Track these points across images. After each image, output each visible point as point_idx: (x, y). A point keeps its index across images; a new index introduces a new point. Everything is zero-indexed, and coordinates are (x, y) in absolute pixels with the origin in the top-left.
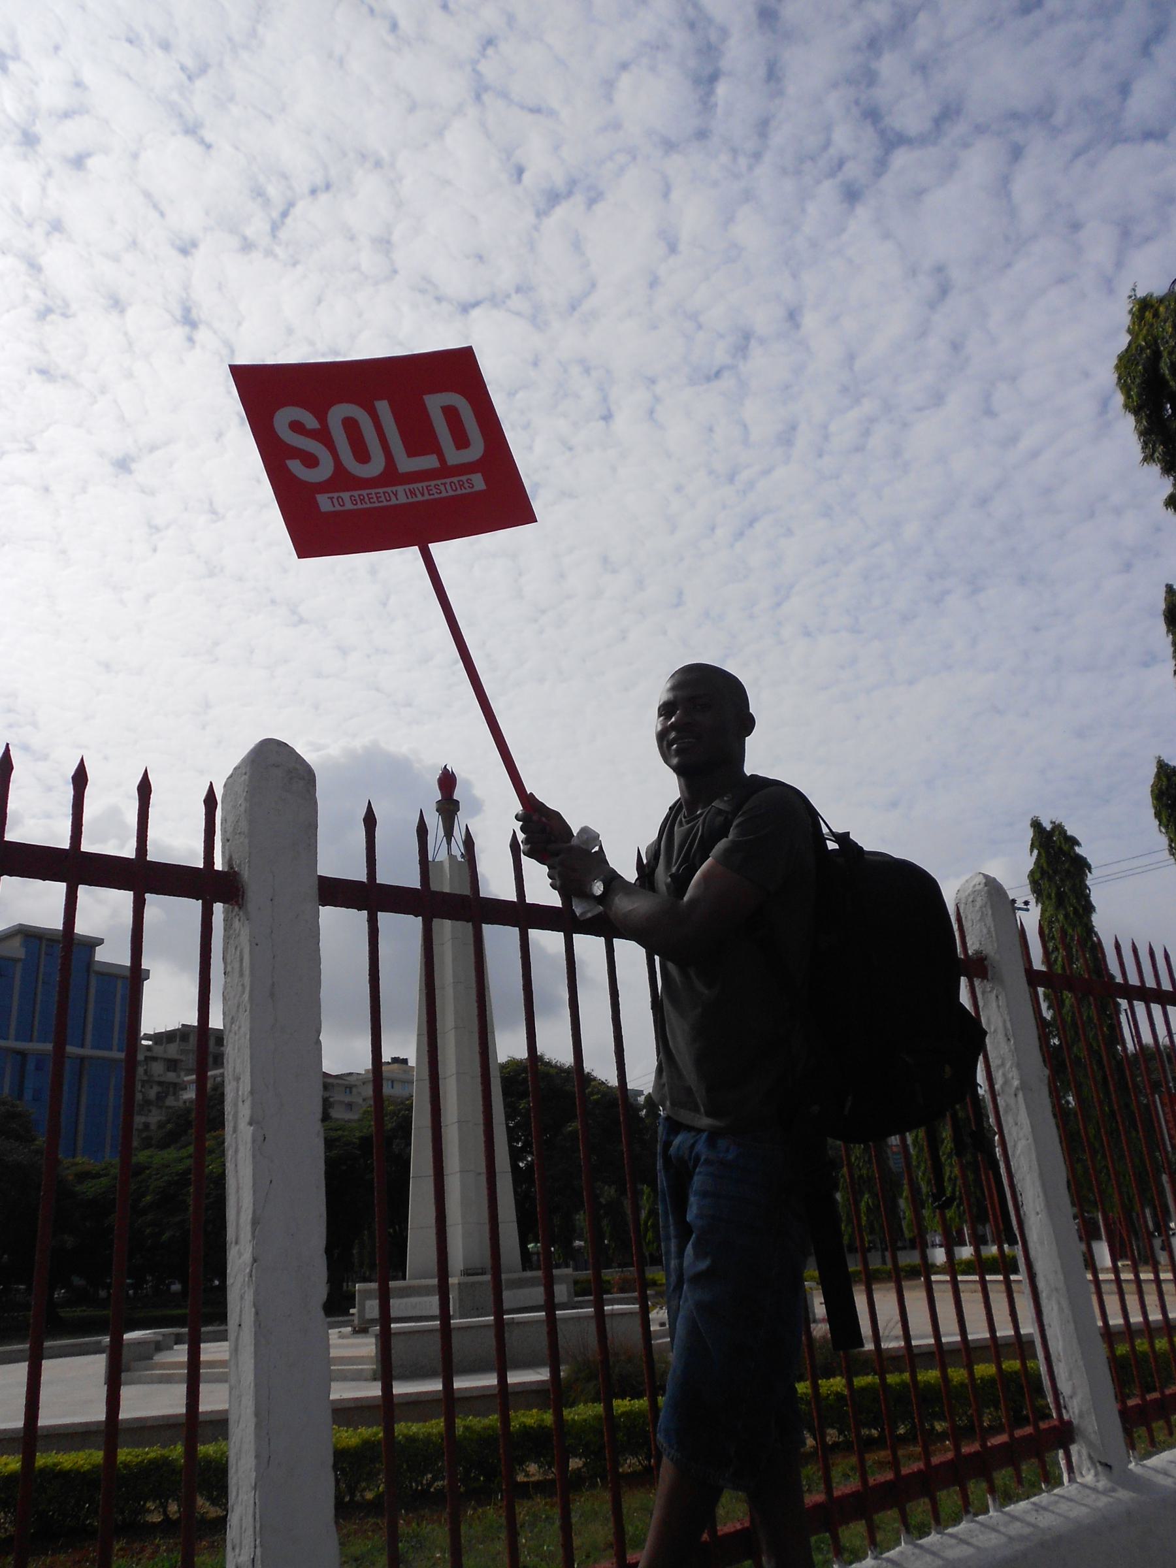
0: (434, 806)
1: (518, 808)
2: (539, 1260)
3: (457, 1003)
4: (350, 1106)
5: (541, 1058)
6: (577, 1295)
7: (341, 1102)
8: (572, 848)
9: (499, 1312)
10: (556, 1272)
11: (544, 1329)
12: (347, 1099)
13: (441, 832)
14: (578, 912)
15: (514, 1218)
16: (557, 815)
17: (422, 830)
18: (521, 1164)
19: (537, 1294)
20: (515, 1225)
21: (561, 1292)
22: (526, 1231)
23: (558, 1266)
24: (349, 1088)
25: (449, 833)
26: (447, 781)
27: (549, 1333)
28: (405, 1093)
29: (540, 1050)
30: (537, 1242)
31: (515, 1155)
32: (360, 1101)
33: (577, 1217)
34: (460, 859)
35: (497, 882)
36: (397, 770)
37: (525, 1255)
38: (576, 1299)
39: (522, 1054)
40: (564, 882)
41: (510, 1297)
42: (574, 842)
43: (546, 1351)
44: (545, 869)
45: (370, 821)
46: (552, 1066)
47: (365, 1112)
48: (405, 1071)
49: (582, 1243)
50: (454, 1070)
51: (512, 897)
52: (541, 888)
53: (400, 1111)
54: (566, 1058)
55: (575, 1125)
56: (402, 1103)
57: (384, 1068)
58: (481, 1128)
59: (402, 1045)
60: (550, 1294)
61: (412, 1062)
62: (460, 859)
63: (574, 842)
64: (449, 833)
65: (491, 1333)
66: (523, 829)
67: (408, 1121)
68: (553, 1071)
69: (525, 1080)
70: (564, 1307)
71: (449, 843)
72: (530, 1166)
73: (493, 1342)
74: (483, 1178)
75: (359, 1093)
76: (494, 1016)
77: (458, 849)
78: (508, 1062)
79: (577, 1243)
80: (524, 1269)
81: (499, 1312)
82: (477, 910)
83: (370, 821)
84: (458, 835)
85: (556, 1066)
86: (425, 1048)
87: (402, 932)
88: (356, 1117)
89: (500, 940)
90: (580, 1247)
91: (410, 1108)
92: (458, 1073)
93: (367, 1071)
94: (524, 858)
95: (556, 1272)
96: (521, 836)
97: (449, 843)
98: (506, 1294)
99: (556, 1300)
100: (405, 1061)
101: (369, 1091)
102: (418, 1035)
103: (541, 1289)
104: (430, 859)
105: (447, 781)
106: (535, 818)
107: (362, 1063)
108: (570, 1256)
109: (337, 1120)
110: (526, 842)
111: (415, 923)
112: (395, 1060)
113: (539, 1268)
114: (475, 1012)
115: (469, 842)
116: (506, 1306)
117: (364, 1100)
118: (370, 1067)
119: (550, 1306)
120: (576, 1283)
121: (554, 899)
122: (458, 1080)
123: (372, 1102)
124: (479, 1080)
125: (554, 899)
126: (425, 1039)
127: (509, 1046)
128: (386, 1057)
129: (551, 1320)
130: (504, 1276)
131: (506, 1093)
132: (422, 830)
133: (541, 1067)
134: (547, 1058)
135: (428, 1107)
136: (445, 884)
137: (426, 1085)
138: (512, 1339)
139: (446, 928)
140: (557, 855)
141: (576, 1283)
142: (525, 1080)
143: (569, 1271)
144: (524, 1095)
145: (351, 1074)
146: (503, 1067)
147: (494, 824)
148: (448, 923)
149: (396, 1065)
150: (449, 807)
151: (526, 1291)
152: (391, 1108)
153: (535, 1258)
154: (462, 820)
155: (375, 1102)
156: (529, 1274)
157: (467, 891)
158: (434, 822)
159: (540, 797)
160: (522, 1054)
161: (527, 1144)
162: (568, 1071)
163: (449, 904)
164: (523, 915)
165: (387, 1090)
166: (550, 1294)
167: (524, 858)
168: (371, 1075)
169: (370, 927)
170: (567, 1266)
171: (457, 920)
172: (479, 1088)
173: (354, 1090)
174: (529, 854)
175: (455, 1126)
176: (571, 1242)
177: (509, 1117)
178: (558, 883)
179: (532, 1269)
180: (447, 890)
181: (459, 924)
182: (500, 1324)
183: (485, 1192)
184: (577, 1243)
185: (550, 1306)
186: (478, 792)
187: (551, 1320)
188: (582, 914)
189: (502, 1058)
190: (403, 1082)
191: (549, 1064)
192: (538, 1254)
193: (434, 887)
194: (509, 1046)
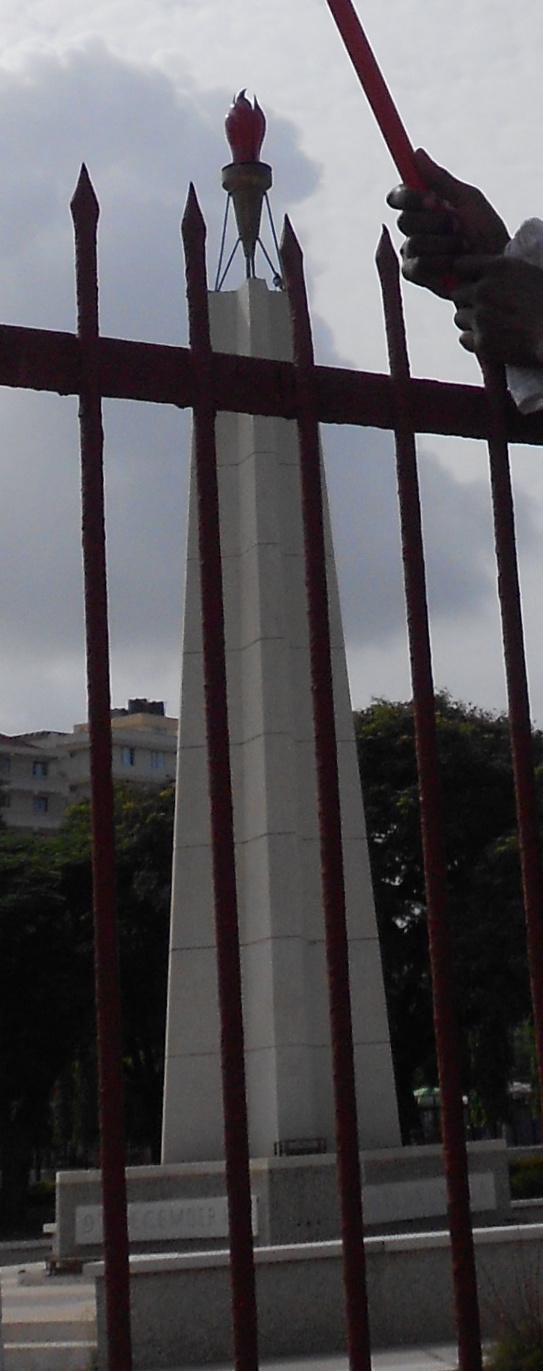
0: (219, 178)
1: (394, 181)
2: (436, 1122)
3: (261, 586)
4: (43, 801)
5: (440, 702)
6: (516, 1195)
7: (25, 794)
8: (506, 265)
9: (353, 1230)
10: (471, 1146)
11: (448, 1266)
12: (38, 787)
13: (234, 232)
14: (518, 396)
15: (386, 1035)
16: (474, 196)
17: (194, 228)
18: (399, 923)
19: (434, 1192)
20: (387, 1049)
21: (483, 1188)
22: (408, 1066)
23: (476, 1135)
24: (42, 764)
25: (249, 234)
26: (246, 124)
27: (457, 1273)
28: (158, 775)
29: (438, 686)
30: (432, 1084)
31: (387, 904)
32: (65, 791)
33: (517, 1032)
34: (272, 287)
35: (349, 338)
36: (143, 101)
37: (409, 1111)
38: (514, 1203)
39: (402, 692)
40: (486, 334)
41: (375, 1199)
42: (510, 251)
43: (452, 1312)
44: (450, 308)
45: (85, 207)
46: (464, 719)
47: (76, 814)
48: (158, 730)
49: (527, 1087)
50: (259, 728)
51: (379, 364)
52: (442, 350)
53: (147, 811)
54: (494, 703)
55: (512, 841)
56: (153, 795)
57: (115, 722)
58: (316, 847)
59: (153, 673)
60: (459, 1191)
61: (173, 711)
62: (272, 287)
63: (510, 251)
64: (249, 234)
65: (338, 1275)
66: (403, 225)
67: (164, 832)
68: (465, 729)
69: (408, 747)
70: (490, 1219)
71: (250, 254)
72: (418, 926)
73: (342, 1293)
74: (322, 951)
75: (63, 775)
76: (343, 604)
77: (268, 267)
78: (372, 710)
79: (517, 1087)
80: (406, 1141)
81: (353, 1230)
82: (305, 393)
83: (85, 207)
84: (269, 238)
85: (472, 719)
86: (201, 680)
87: (150, 437)
88: (56, 824)
89: (357, 454)
90: (523, 1095)
91: (168, 806)
92: (267, 733)
93: (79, 728)
94: (405, 285)
95: (471, 1146)
96: (399, 240)
97: (250, 254)
98: (369, 1193)
99: (474, 1206)
100: (158, 708)
101: (82, 769)
102: (186, 654)
103: (442, 1183)
104: (211, 287)
105: (246, 124)
106: (429, 200)
107: (70, 713)
108: (502, 1113)
109: (17, 830)
110: (411, 251)
111: (178, 421)
112: (138, 706)
113: (435, 1139)
114: (304, 605)
115: (291, 253)
116: (368, 1217)
117: (73, 788)
118: (85, 720)
119: (460, 1217)
120: (514, 1169)
121: (467, 371)
122: (268, 747)
123: (88, 793)
124: (312, 747)
125: (467, 371)
126: (200, 661)
127: (375, 677)
128: (119, 700)
129: (463, 1245)
130: (363, 1156)
131: (369, 773)
132: (194, 228)
133: (440, 720)
134: (453, 701)
135: (206, 804)
136: (240, 338)
137: (203, 757)
138: (381, 1285)
139: (242, 431)
140: (475, 280)
141: (514, 1169)
142: (408, 747)
143: (500, 1144)
144: (406, 778)
145: (45, 735)
146: (362, 719)
147: (341, 214)
148: (247, 421)
149: (139, 717)
150: (249, 180)
151: (409, 1187)
152: (130, 805)
153: (428, 1117)
154: (277, 205)
155: (95, 793)
156: (415, 1151)
157: (287, 355)
158: (219, 210)
159: (440, 158)
160: (402, 692)
161: (412, 881)
162: (496, 729)
163: (251, 381)
164: (403, 404)
165: (120, 768)
166: (459, 1191)
167: (405, 285)
168: (86, 737)
169: (85, 429)
170: (496, 1135)
171: (266, 413)
172: (313, 763)
173: (53, 768)
174: (416, 278)
175: (262, 846)
176: (502, 1085)
177: (374, 824)
178: (477, 338)
179: (422, 1140)
180: (245, 350)
181: (273, 422)
182: (355, 1257)
183: (324, 980)
184: (517, 1087)
185: (460, 1217)
186: (312, 146)
187: (463, 1245)
188: (525, 402)
189: (360, 699)
190: (155, 751)
191: (457, 714)
192: (434, 1108)
193: (218, 345)
194: (375, 677)
